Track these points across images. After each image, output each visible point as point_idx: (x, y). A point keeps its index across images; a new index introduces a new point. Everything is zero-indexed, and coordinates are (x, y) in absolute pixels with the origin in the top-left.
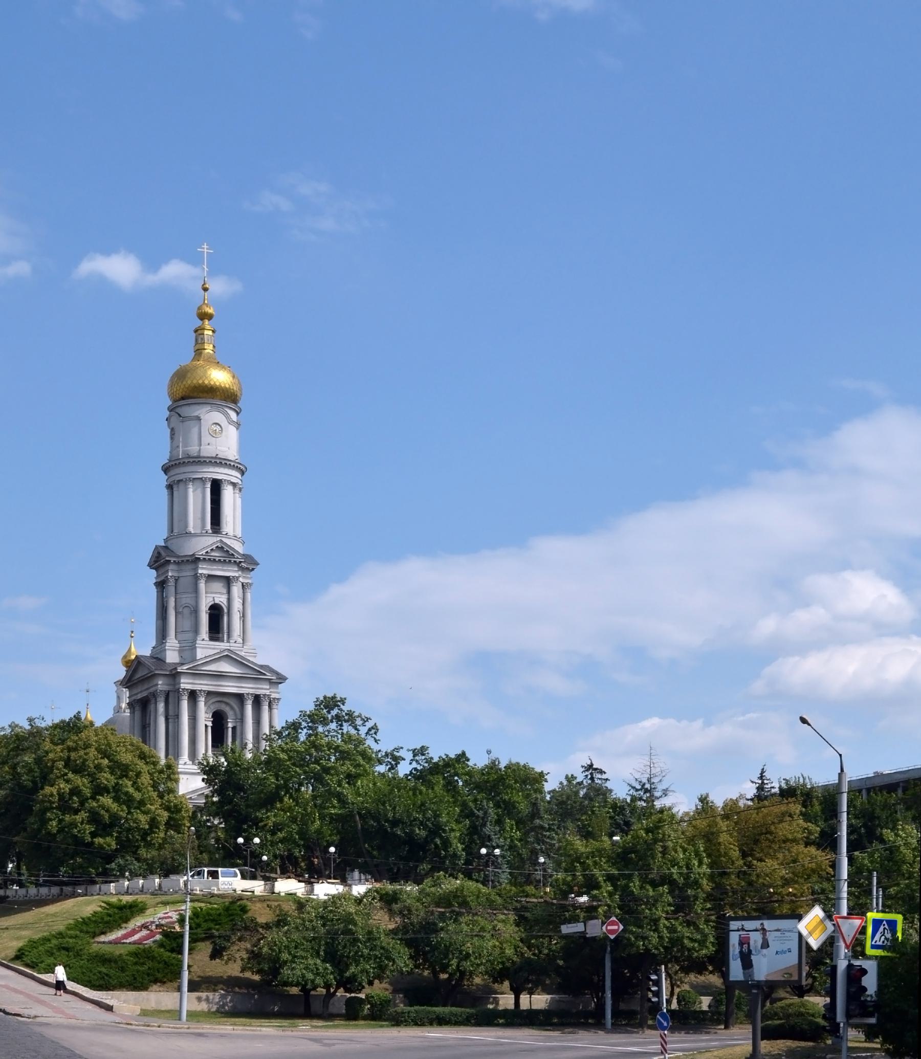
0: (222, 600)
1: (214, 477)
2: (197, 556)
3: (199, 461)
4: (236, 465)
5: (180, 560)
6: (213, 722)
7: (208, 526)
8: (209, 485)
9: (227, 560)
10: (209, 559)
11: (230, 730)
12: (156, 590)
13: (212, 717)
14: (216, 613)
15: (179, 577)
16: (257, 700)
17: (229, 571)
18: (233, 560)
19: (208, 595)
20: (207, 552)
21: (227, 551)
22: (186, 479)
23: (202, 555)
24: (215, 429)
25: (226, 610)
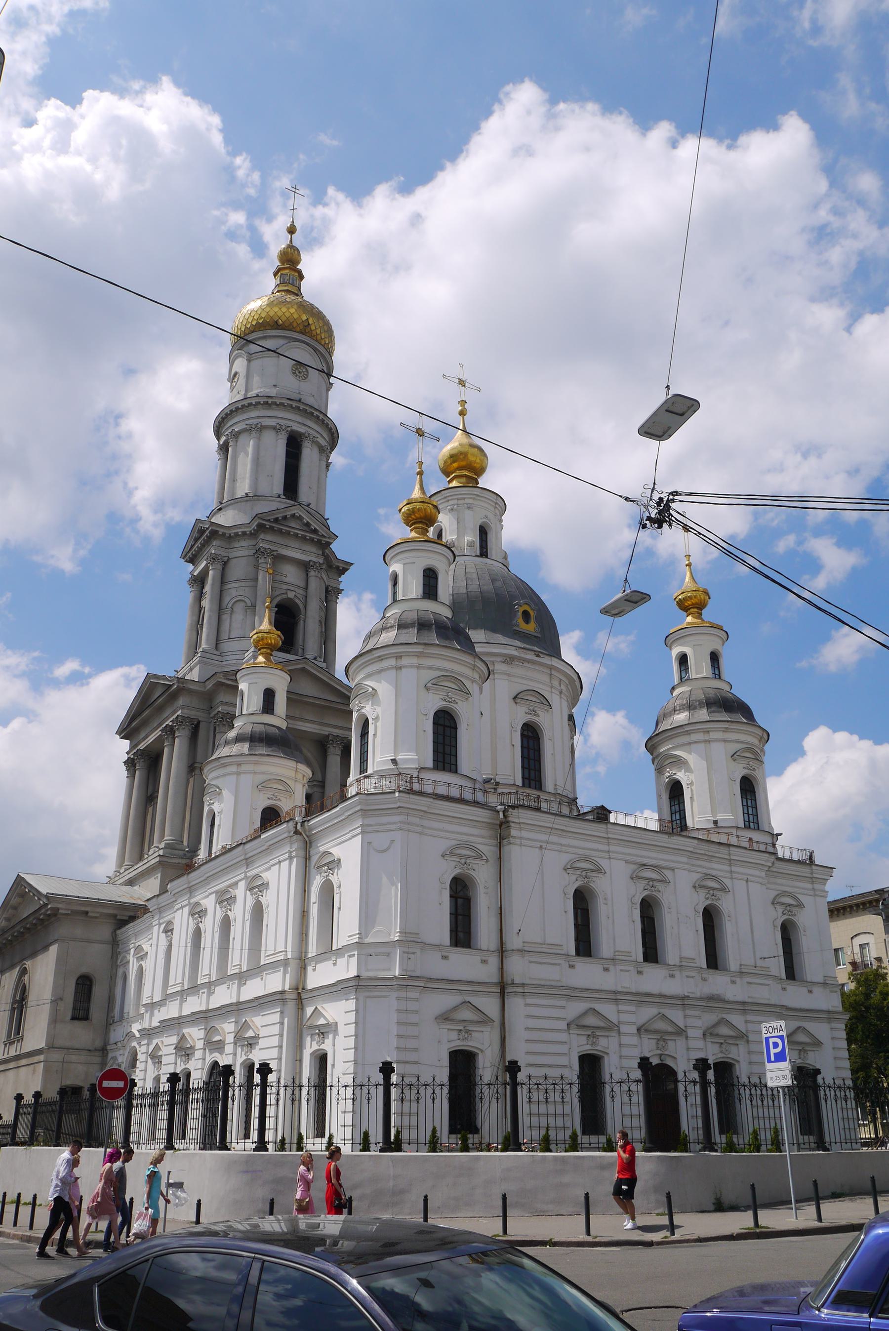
1: (294, 428)
20: (276, 520)
21: (308, 525)
23: (269, 521)
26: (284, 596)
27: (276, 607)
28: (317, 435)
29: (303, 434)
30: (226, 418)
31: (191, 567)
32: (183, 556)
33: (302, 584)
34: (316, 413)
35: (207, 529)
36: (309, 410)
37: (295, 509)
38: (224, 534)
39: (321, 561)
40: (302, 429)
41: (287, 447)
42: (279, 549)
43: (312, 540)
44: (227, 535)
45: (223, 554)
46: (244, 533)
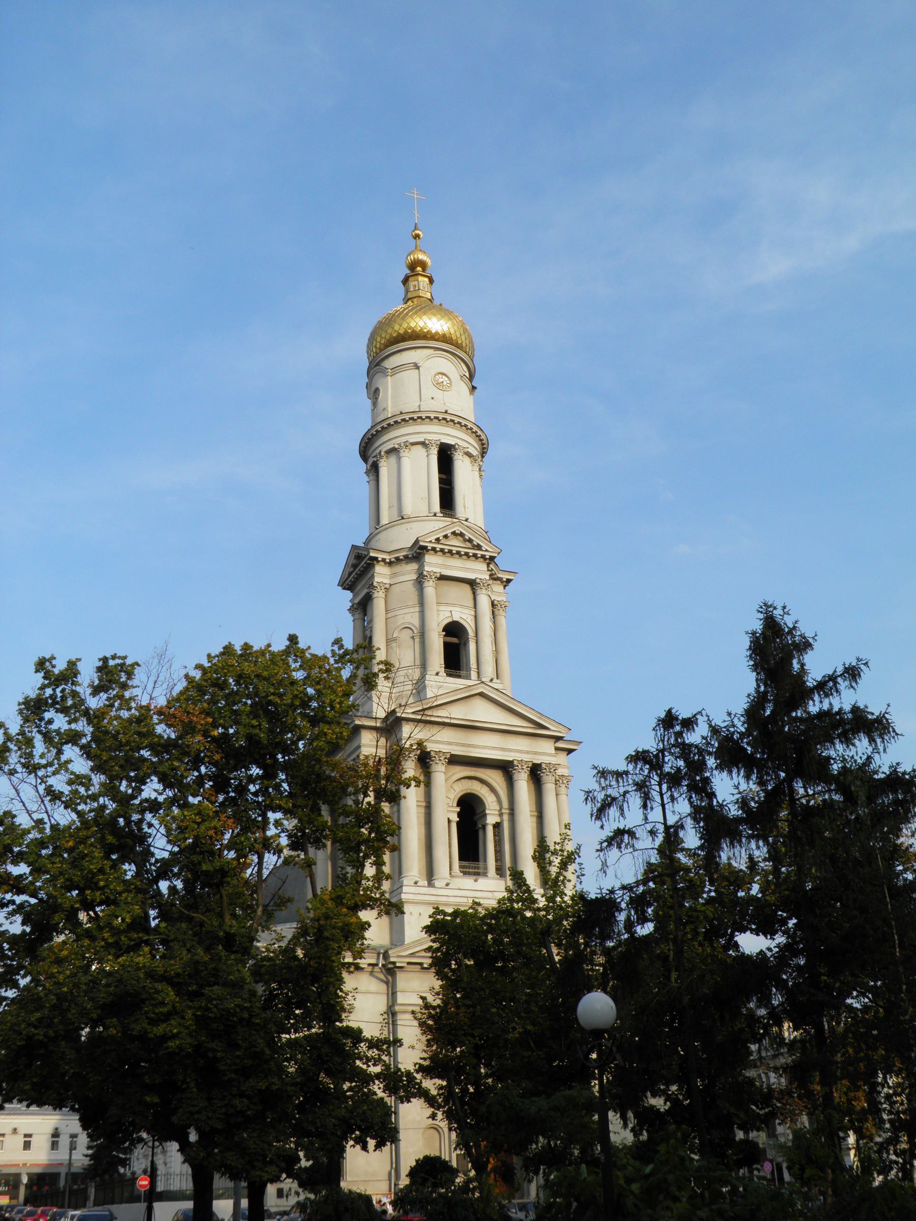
0: (464, 616)
1: (443, 441)
2: (421, 543)
3: (419, 418)
4: (475, 429)
5: (392, 557)
6: (459, 815)
7: (436, 506)
8: (434, 451)
9: (471, 552)
10: (442, 550)
11: (490, 831)
12: (352, 618)
13: (458, 805)
14: (454, 630)
15: (391, 585)
16: (536, 773)
17: (474, 571)
18: (479, 553)
19: (442, 608)
20: (438, 540)
21: (470, 541)
22: (400, 444)
23: (430, 542)
24: (441, 380)
25: (471, 634)
28: (468, 445)
29: (453, 446)
33: (471, 604)
34: (464, 422)
35: (366, 556)
36: (456, 420)
37: (454, 527)
38: (384, 560)
39: (488, 578)
44: (388, 561)
45: (387, 581)
46: (406, 557)
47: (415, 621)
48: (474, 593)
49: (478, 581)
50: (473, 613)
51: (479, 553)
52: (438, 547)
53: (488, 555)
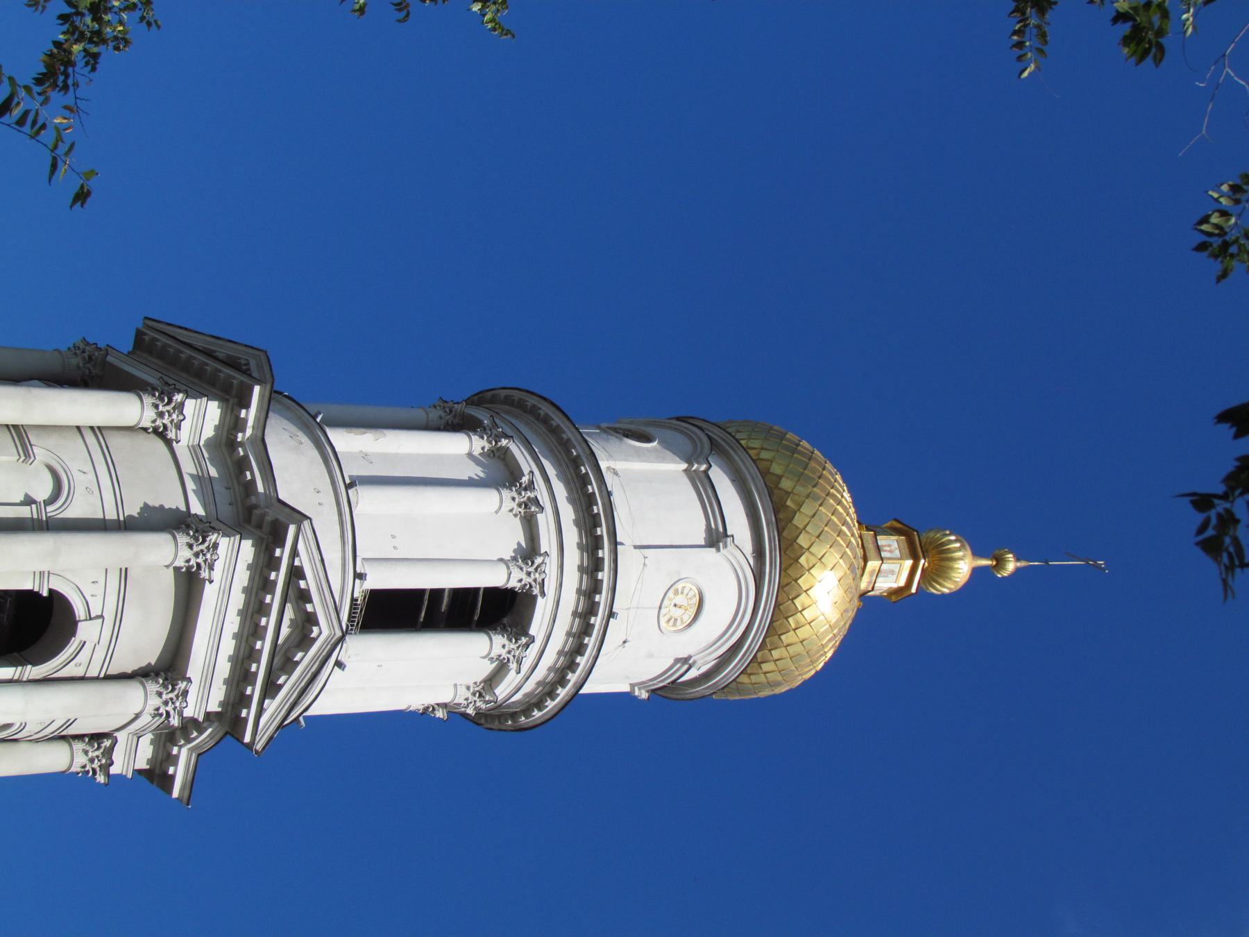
1: (540, 602)
18: (255, 691)
20: (296, 573)
21: (288, 665)
23: (294, 553)
26: (79, 611)
27: (51, 591)
30: (538, 417)
31: (127, 345)
32: (150, 323)
36: (591, 642)
38: (239, 425)
39: (188, 713)
40: (537, 627)
41: (487, 590)
42: (216, 585)
43: (249, 678)
47: (78, 508)
48: (143, 674)
49: (182, 685)
50: (93, 672)
51: (255, 691)
52: (279, 577)
53: (249, 714)
